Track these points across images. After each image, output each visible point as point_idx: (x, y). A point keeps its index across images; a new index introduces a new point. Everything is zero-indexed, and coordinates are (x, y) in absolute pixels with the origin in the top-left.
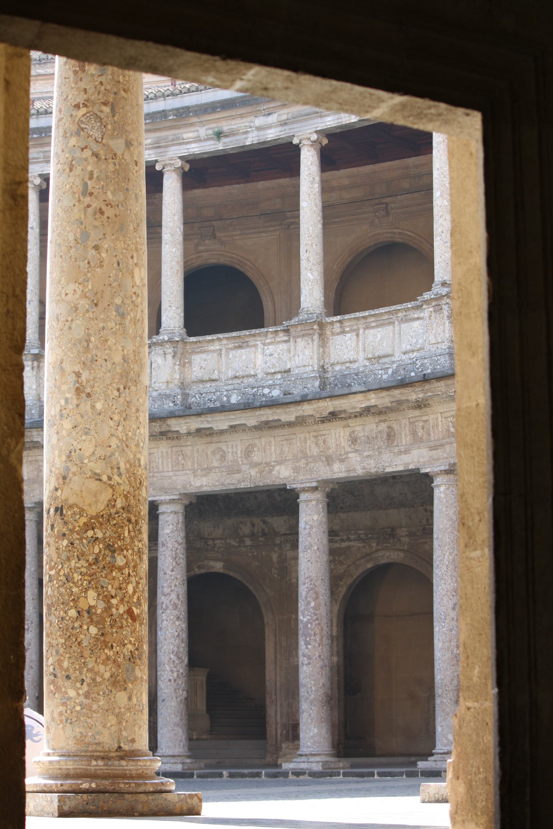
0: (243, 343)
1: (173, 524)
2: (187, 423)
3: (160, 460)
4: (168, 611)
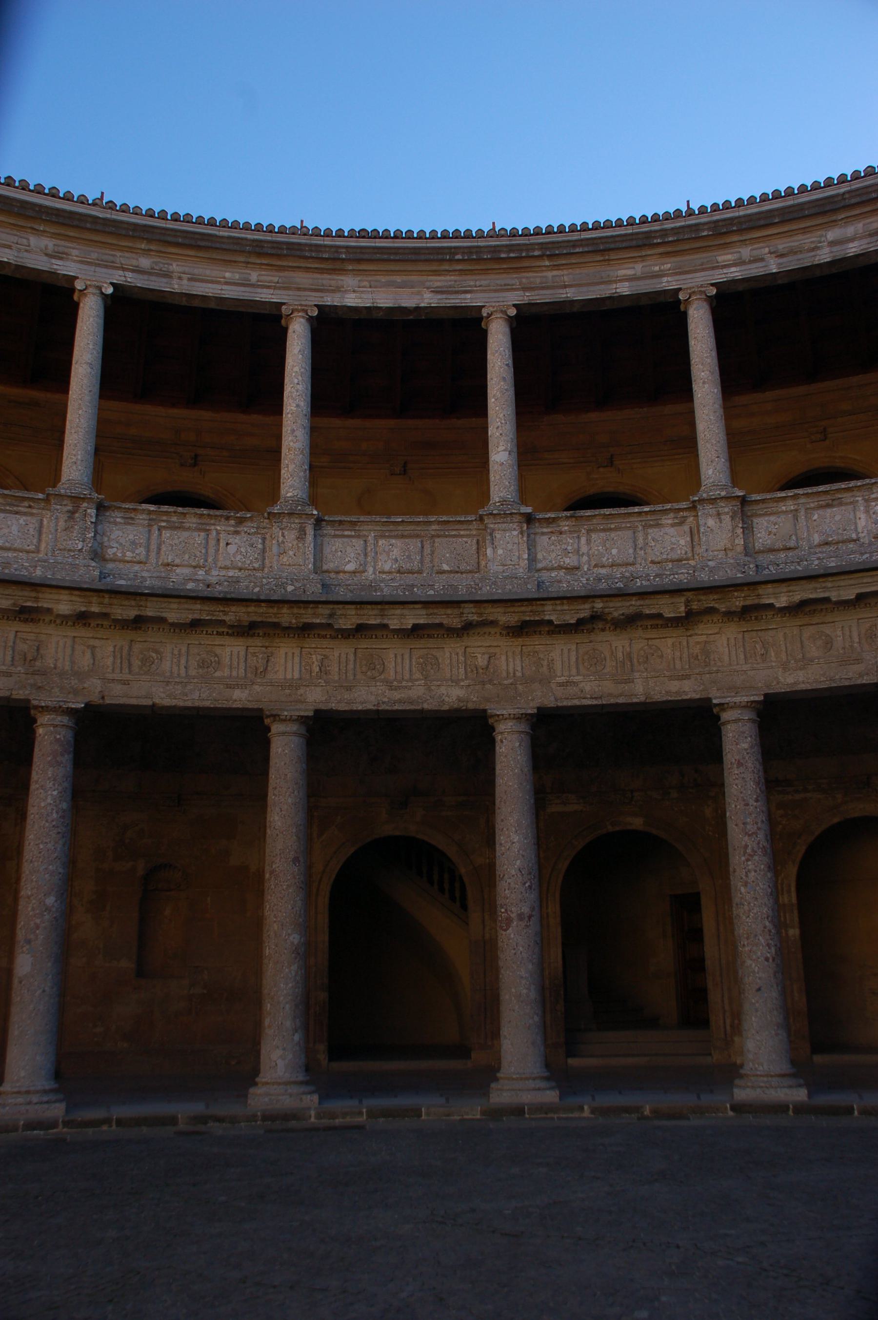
0: (833, 500)
1: (751, 736)
2: (790, 592)
3: (727, 650)
4: (756, 858)
